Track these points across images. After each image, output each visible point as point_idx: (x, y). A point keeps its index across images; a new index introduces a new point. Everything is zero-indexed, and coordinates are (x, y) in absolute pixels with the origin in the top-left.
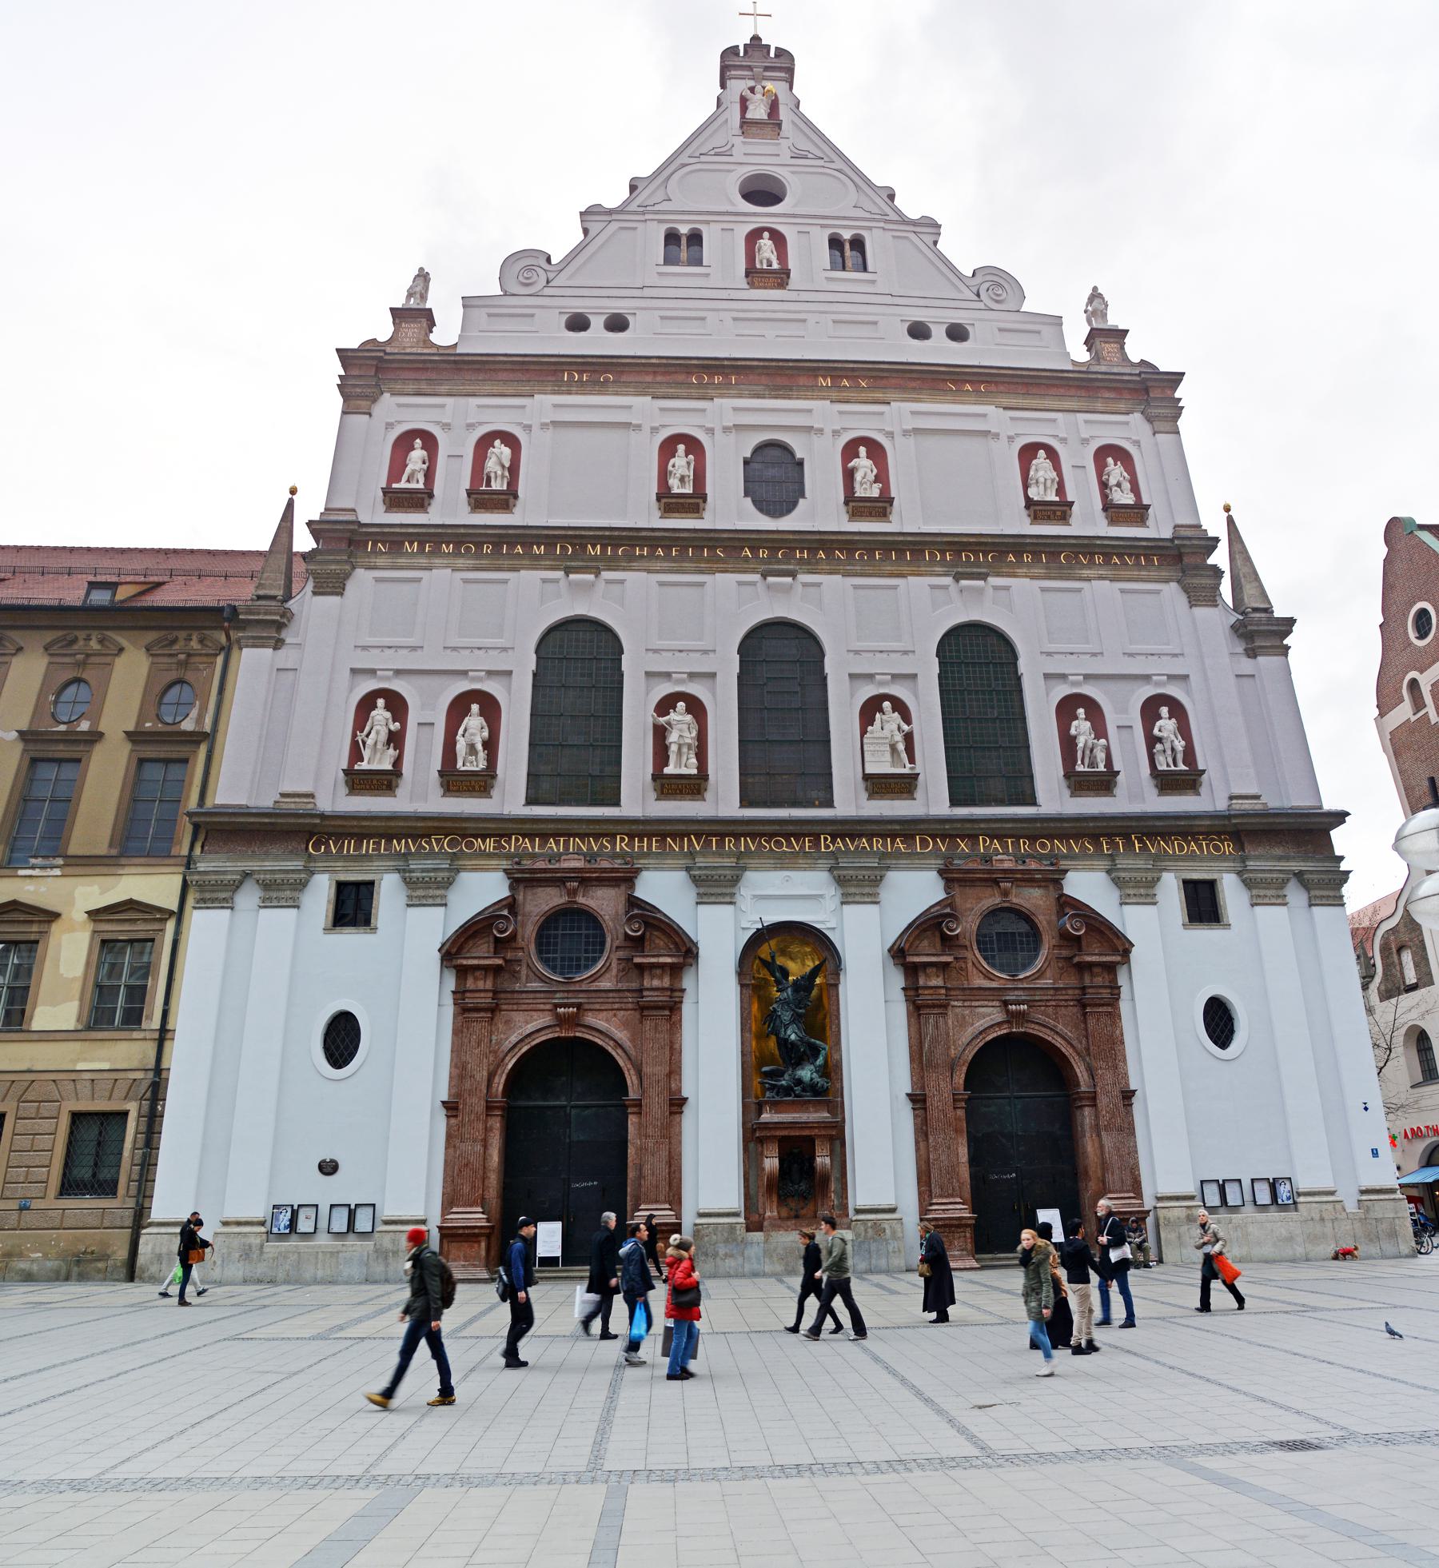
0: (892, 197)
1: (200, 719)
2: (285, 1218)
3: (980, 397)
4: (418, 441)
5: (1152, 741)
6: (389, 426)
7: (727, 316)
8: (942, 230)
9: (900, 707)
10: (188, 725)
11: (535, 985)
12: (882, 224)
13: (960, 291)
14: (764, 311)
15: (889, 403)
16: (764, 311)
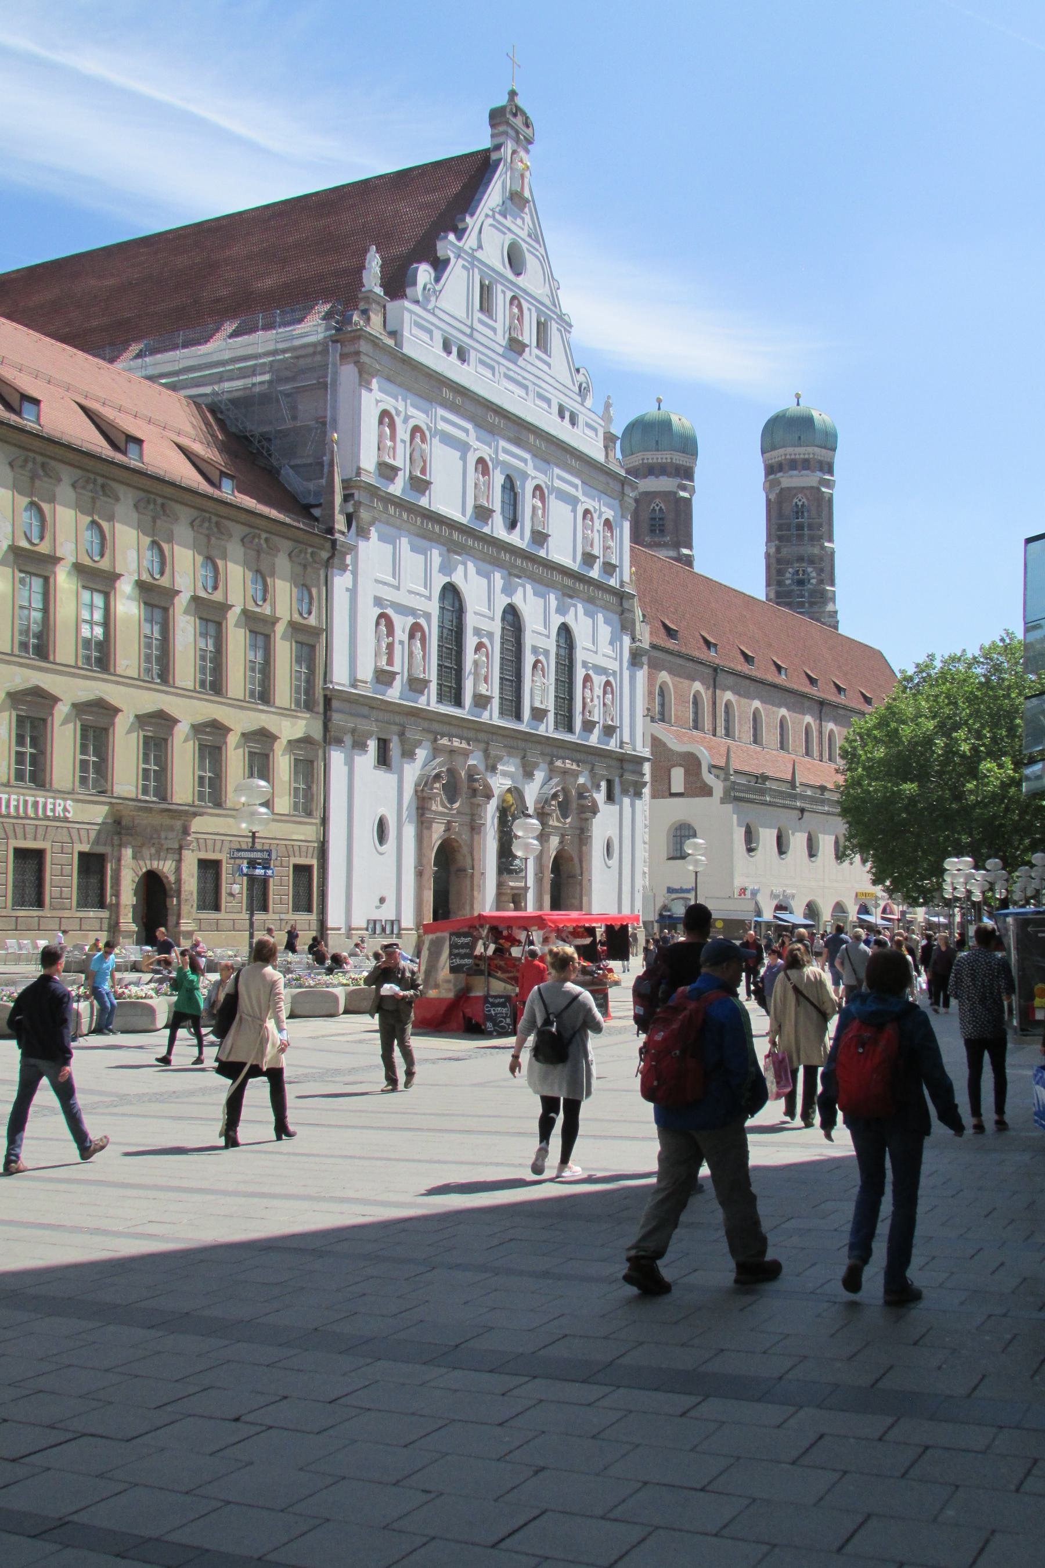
0: (558, 289)
1: (319, 616)
2: (371, 926)
3: (577, 474)
4: (387, 420)
5: (604, 704)
6: (378, 402)
7: (503, 370)
8: (573, 330)
9: (543, 670)
10: (312, 621)
11: (441, 809)
12: (555, 317)
13: (574, 384)
14: (515, 372)
15: (549, 463)
16: (515, 372)
